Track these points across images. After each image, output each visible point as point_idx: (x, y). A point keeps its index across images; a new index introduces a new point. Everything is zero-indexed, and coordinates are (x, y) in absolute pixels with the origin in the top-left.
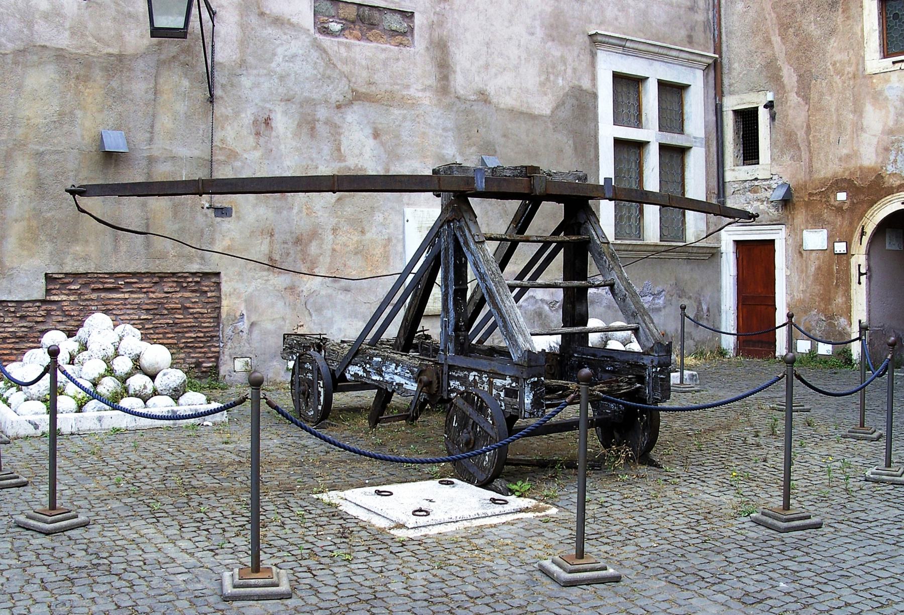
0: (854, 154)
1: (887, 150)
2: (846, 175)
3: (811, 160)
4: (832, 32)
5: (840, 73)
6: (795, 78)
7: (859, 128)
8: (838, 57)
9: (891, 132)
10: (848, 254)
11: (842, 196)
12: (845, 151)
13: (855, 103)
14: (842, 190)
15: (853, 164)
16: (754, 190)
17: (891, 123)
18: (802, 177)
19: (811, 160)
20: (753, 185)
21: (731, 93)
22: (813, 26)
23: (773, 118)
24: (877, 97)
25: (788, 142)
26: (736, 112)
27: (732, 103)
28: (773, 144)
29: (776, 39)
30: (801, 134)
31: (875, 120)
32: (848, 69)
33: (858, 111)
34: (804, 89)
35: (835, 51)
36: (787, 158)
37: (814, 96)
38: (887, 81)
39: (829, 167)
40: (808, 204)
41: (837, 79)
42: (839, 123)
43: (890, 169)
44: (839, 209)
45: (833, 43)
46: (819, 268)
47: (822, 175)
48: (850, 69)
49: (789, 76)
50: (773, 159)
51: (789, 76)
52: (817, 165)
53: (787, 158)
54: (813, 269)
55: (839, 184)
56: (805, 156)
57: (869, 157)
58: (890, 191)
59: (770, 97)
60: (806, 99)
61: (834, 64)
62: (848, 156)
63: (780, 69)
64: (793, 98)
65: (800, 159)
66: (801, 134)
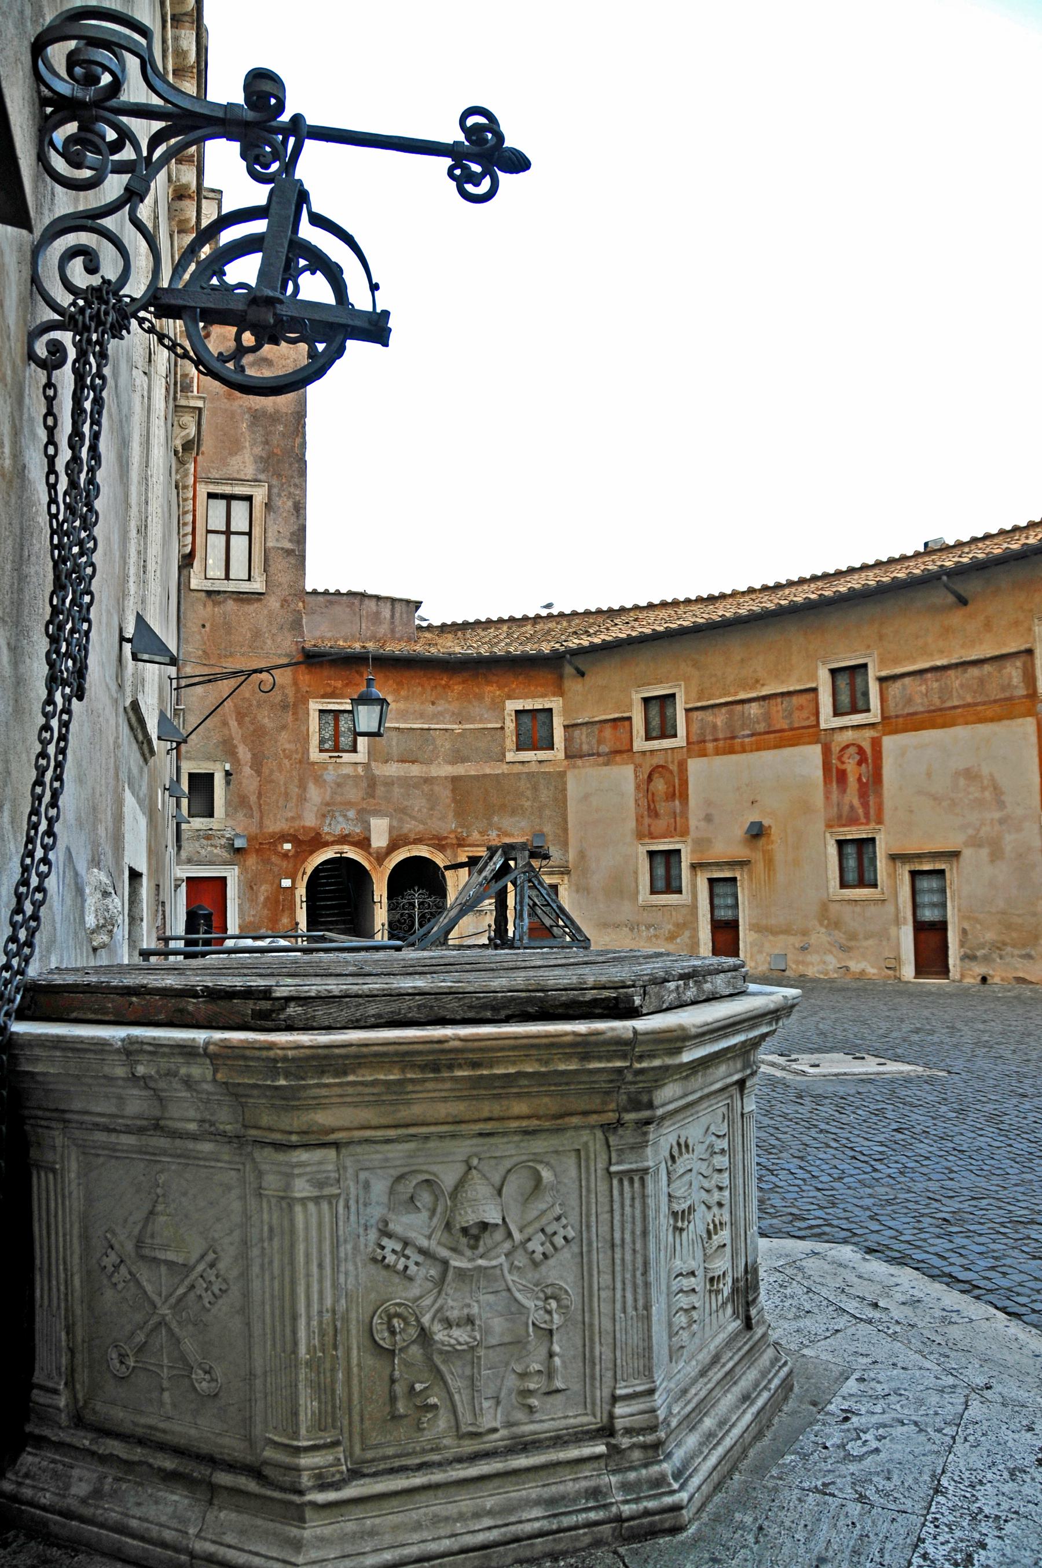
0: (300, 817)
1: (324, 816)
2: (292, 831)
3: (261, 818)
4: (284, 727)
5: (289, 757)
6: (249, 756)
7: (302, 799)
8: (287, 746)
9: (328, 804)
10: (293, 888)
11: (287, 846)
12: (290, 814)
13: (301, 780)
14: (288, 842)
15: (296, 824)
16: (208, 838)
17: (328, 798)
18: (254, 830)
19: (261, 818)
20: (208, 836)
21: (189, 759)
22: (266, 720)
23: (228, 783)
24: (319, 781)
25: (238, 803)
26: (190, 775)
27: (188, 767)
28: (228, 803)
29: (233, 724)
30: (253, 799)
31: (314, 794)
32: (295, 756)
33: (303, 786)
34: (257, 764)
35: (284, 741)
36: (240, 815)
37: (265, 771)
38: (326, 769)
39: (276, 825)
40: (258, 851)
41: (286, 761)
42: (286, 794)
43: (326, 829)
44: (285, 855)
45: (284, 735)
46: (267, 898)
47: (271, 830)
48: (299, 756)
49: (244, 753)
50: (227, 815)
51: (244, 753)
52: (267, 822)
53: (240, 815)
54: (262, 898)
55: (284, 838)
56: (256, 814)
57: (310, 820)
58: (327, 844)
59: (228, 767)
60: (259, 773)
61: (284, 751)
62: (293, 818)
63: (236, 747)
64: (247, 771)
65: (252, 816)
66: (253, 799)
